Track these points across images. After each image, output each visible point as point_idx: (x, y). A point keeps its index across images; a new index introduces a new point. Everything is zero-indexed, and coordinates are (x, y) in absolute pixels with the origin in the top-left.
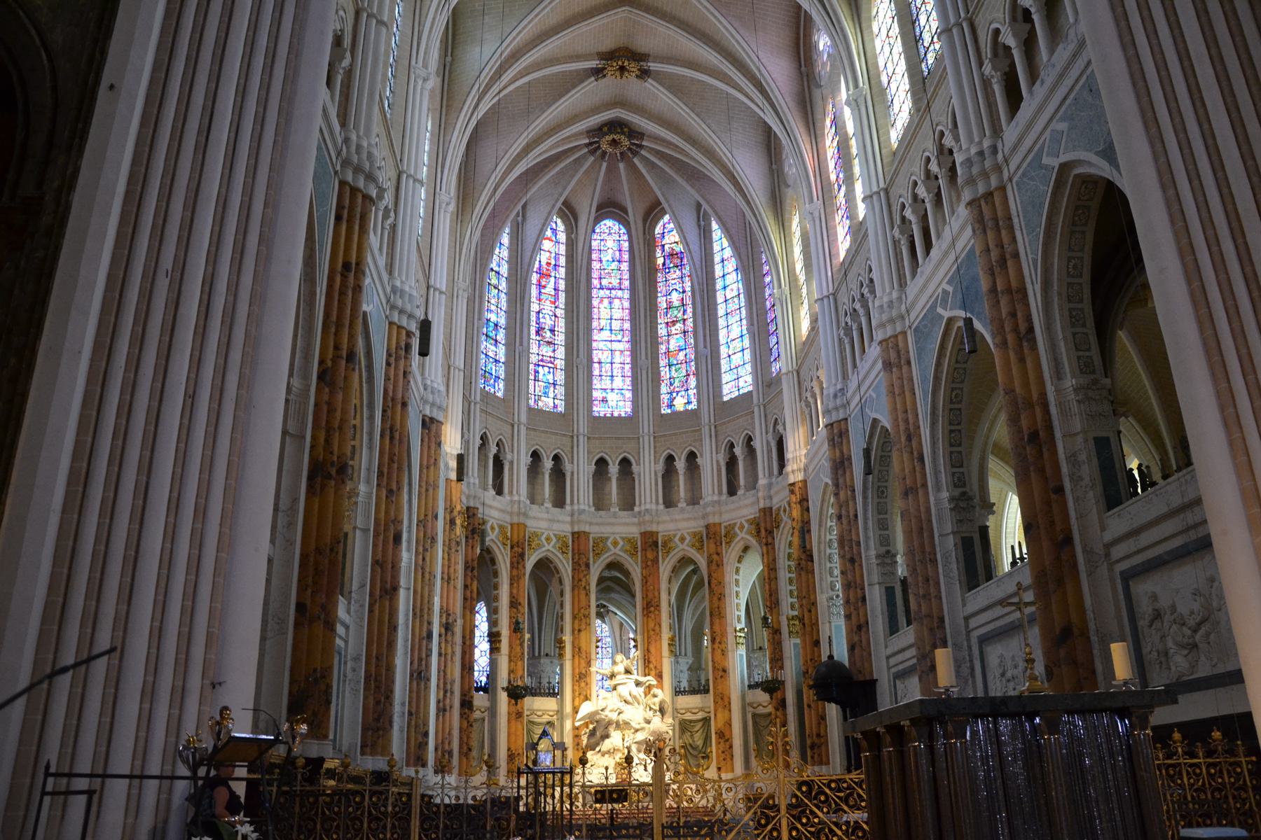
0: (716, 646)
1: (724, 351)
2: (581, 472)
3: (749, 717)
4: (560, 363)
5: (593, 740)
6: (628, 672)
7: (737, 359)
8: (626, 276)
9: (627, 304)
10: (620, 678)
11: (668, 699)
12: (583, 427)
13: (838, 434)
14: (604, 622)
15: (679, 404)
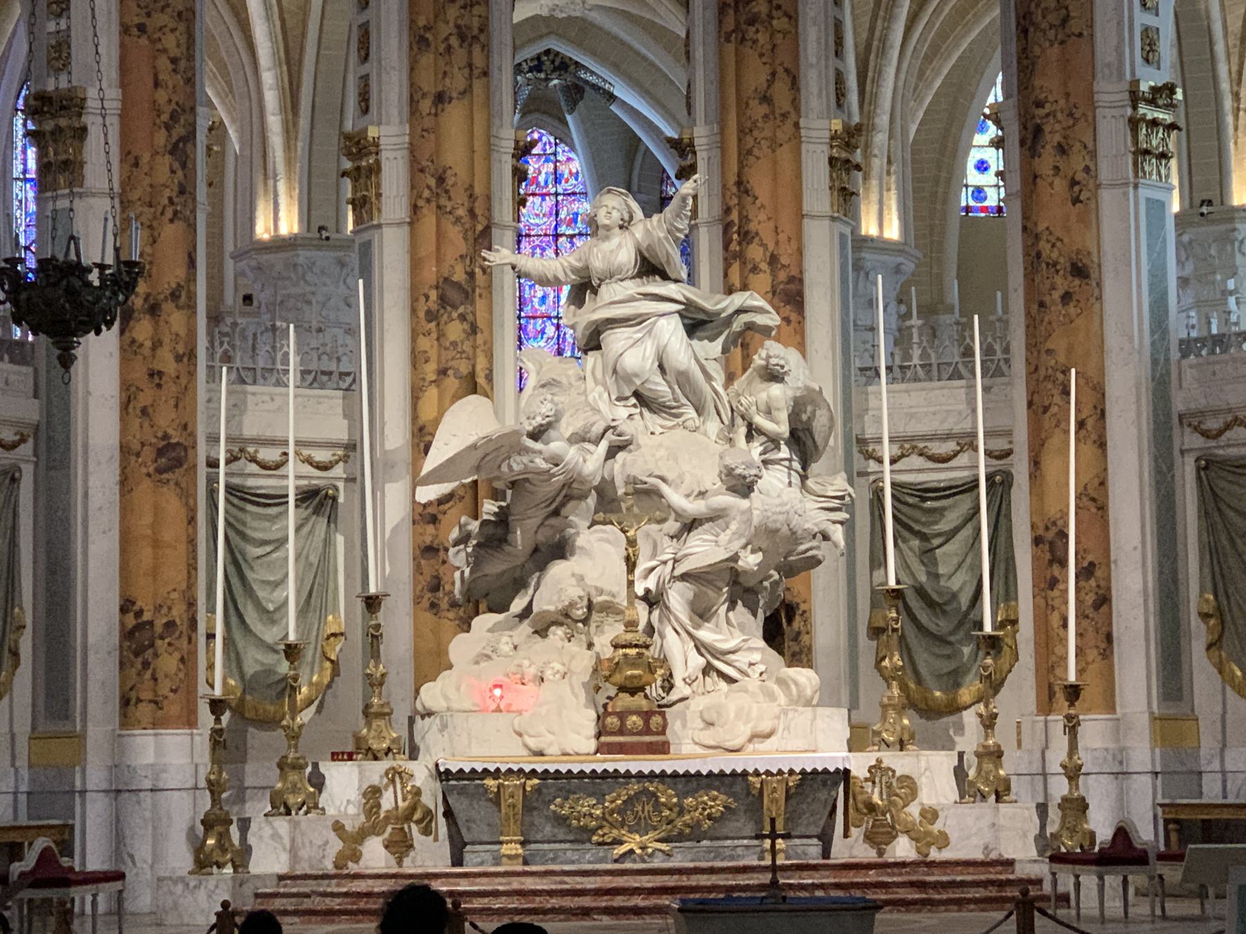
0: (1047, 161)
3: (1187, 471)
5: (497, 566)
6: (649, 267)
10: (618, 296)
11: (831, 393)
14: (563, 138)
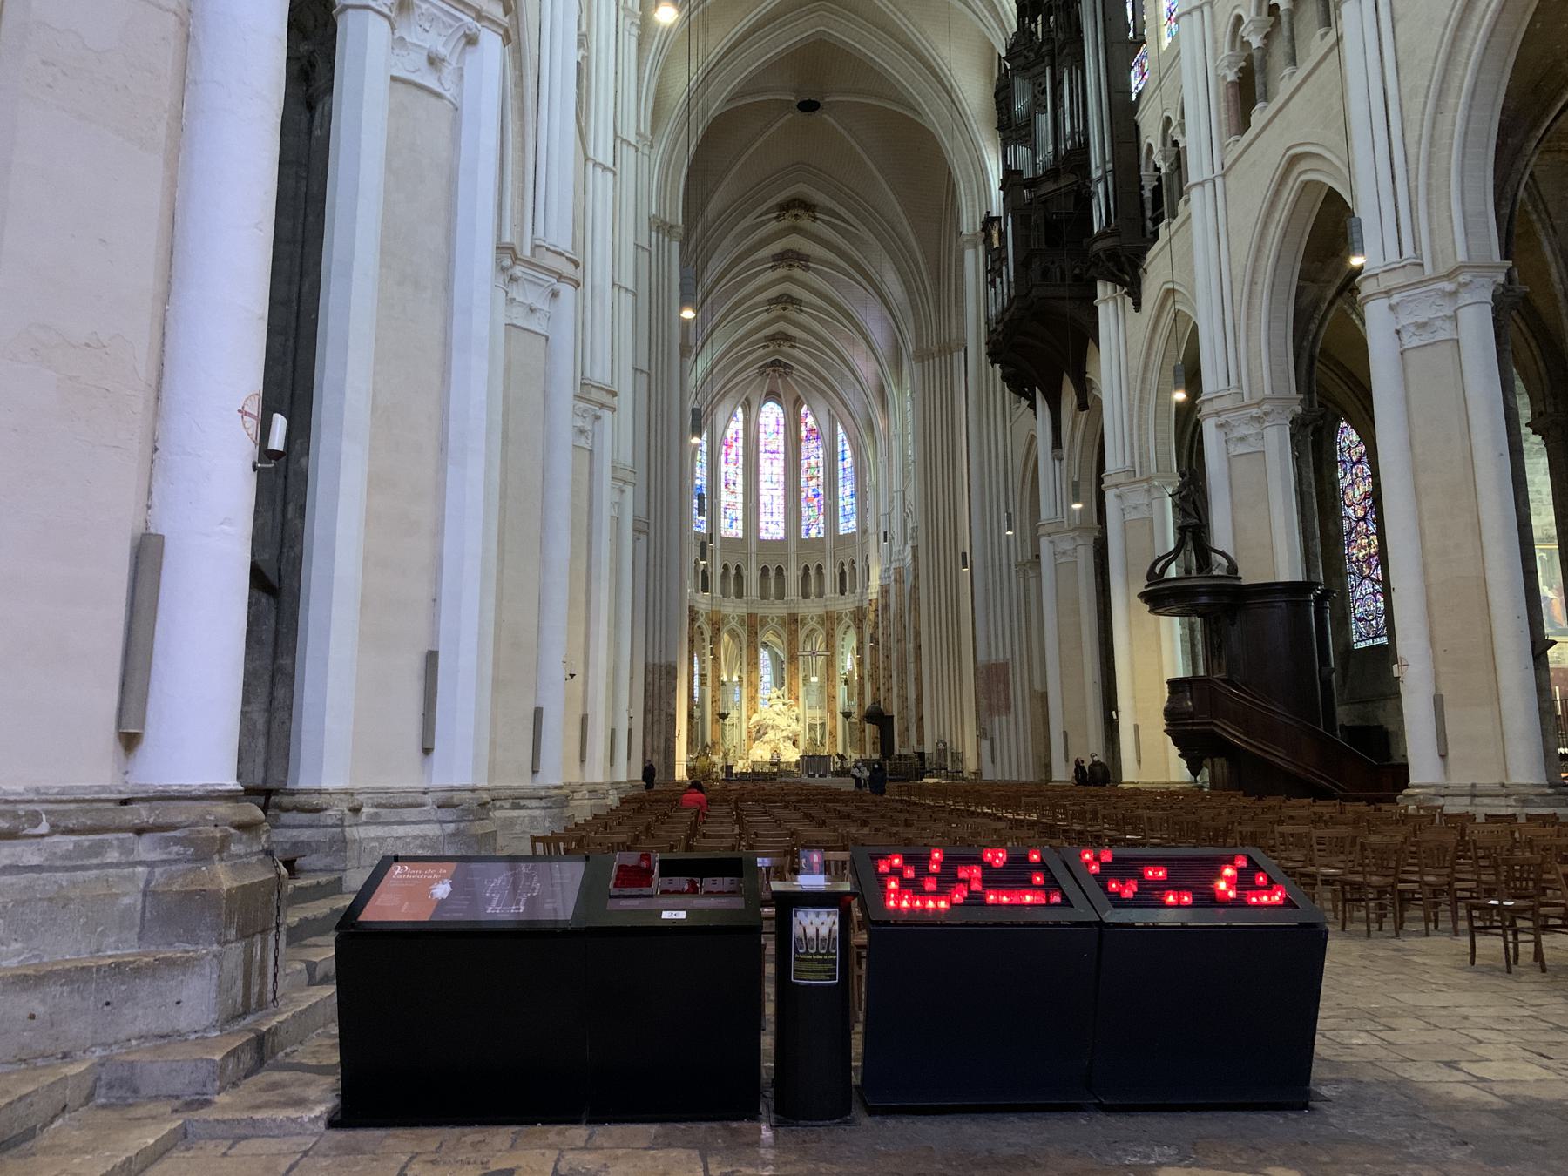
1: (841, 503)
2: (752, 575)
4: (740, 506)
7: (848, 508)
8: (782, 443)
9: (782, 464)
12: (753, 548)
13: (885, 590)
15: (813, 533)
